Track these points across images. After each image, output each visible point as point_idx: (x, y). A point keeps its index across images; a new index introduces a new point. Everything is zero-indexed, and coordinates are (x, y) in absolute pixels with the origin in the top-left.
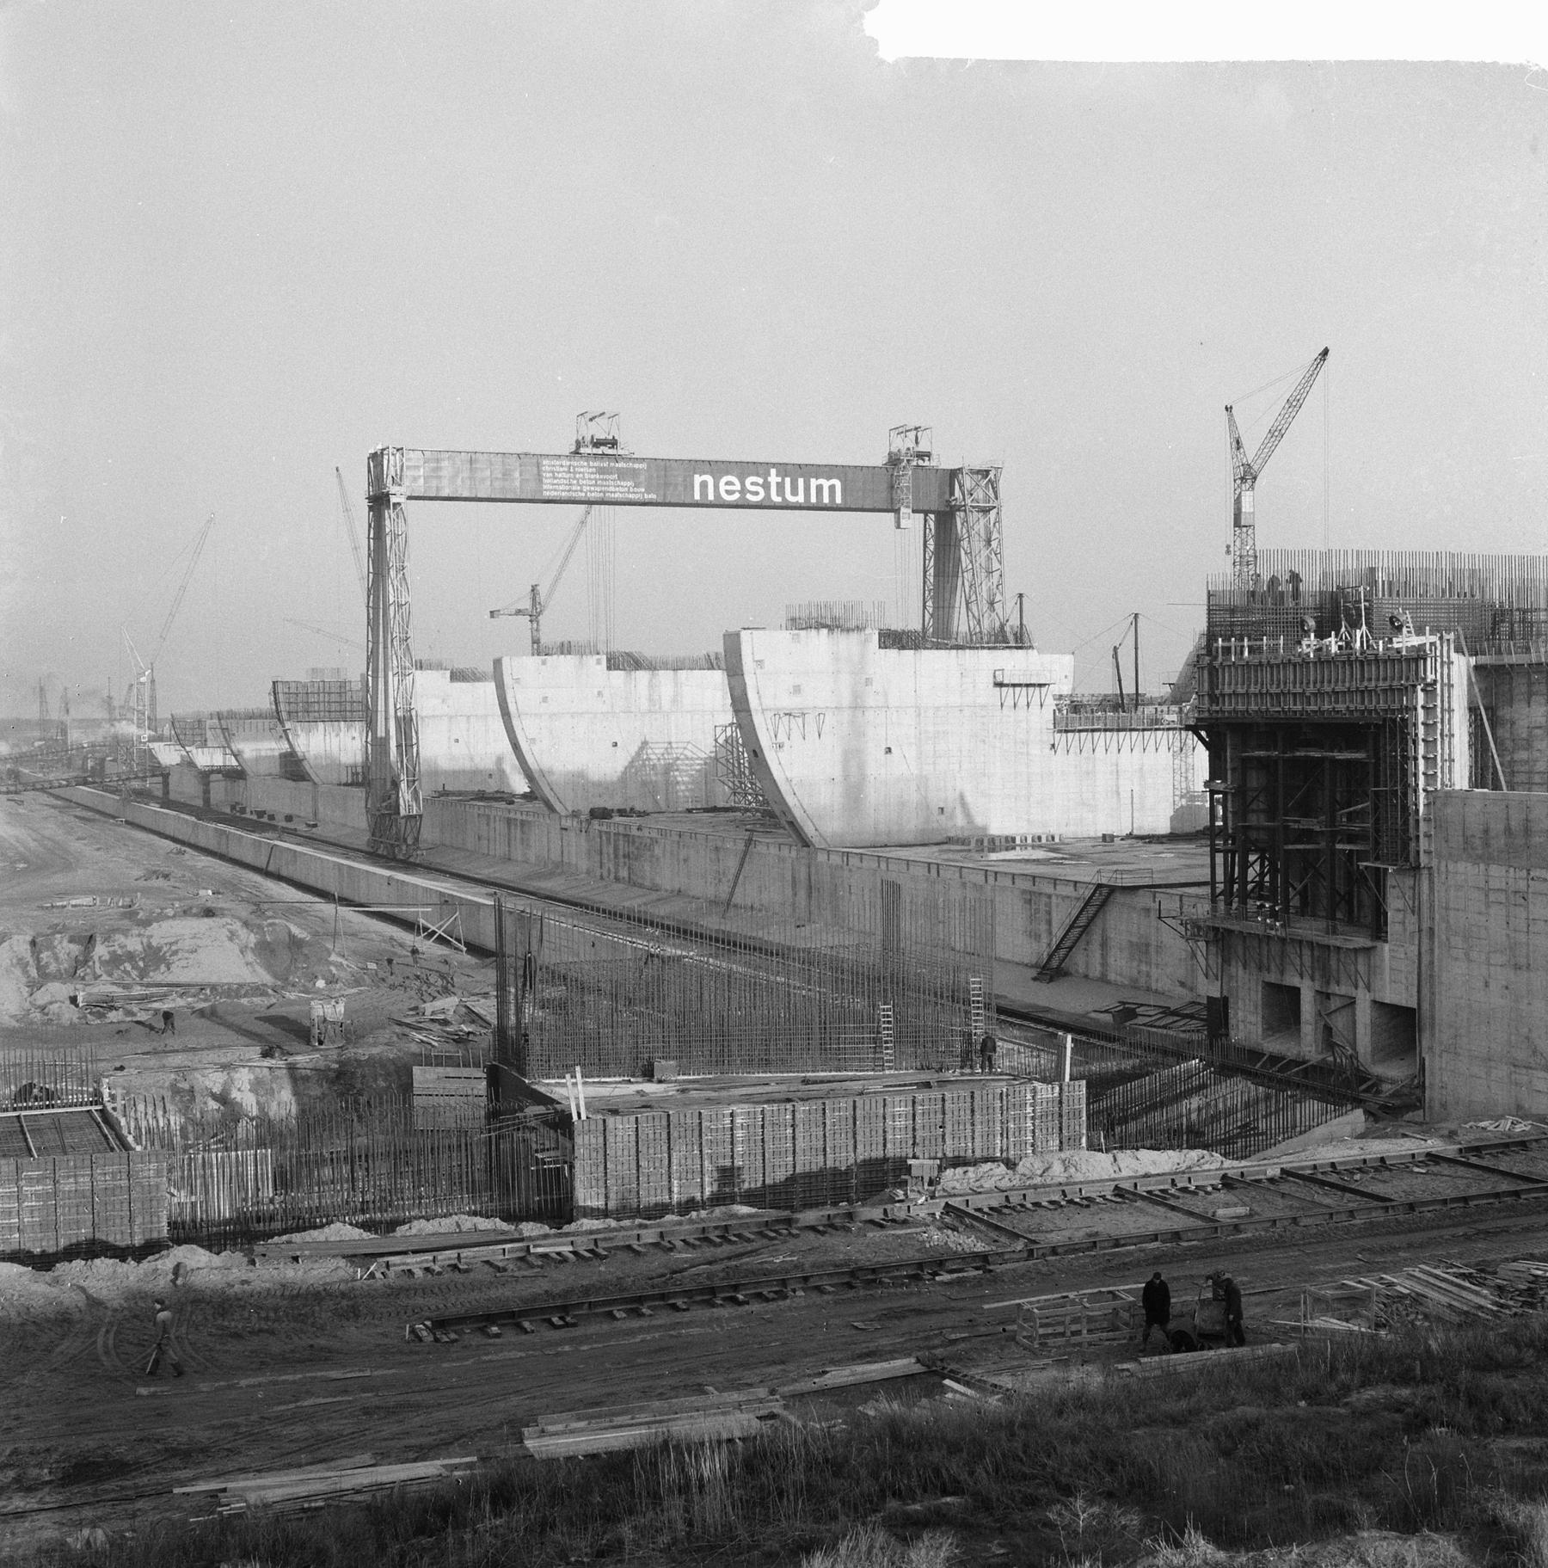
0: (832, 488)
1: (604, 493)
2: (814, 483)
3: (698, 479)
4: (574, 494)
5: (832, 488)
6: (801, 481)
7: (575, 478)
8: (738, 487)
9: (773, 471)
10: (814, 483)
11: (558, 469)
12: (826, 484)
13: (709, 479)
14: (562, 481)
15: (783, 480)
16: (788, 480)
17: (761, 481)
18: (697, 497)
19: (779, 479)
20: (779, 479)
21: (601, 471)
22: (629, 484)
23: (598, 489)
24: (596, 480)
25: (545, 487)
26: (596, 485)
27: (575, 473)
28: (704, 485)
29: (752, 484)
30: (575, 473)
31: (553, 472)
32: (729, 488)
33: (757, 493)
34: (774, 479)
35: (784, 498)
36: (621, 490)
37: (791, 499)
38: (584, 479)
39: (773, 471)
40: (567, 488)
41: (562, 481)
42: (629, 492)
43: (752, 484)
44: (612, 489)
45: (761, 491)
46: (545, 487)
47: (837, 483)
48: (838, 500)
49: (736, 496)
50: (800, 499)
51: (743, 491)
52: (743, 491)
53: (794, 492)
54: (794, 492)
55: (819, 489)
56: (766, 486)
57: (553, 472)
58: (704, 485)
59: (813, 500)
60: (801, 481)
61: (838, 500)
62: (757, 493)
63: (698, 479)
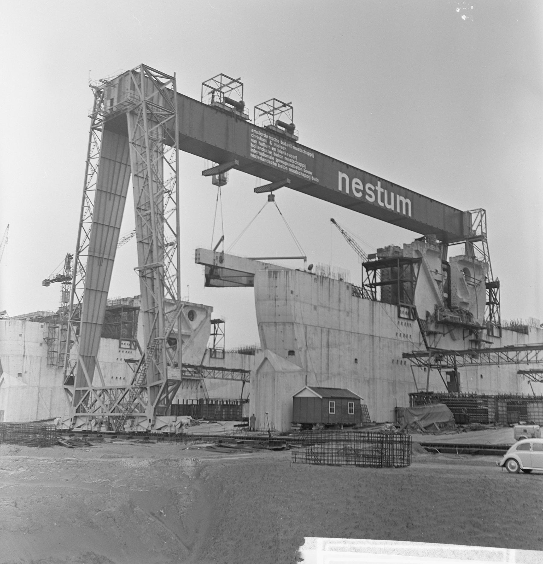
1: (288, 167)
3: (341, 175)
4: (270, 162)
7: (271, 150)
11: (260, 138)
13: (345, 175)
14: (263, 149)
22: (303, 165)
23: (285, 163)
24: (284, 156)
26: (284, 160)
28: (344, 179)
31: (258, 140)
38: (276, 152)
42: (303, 172)
44: (293, 166)
57: (258, 140)
58: (344, 179)
63: (341, 175)
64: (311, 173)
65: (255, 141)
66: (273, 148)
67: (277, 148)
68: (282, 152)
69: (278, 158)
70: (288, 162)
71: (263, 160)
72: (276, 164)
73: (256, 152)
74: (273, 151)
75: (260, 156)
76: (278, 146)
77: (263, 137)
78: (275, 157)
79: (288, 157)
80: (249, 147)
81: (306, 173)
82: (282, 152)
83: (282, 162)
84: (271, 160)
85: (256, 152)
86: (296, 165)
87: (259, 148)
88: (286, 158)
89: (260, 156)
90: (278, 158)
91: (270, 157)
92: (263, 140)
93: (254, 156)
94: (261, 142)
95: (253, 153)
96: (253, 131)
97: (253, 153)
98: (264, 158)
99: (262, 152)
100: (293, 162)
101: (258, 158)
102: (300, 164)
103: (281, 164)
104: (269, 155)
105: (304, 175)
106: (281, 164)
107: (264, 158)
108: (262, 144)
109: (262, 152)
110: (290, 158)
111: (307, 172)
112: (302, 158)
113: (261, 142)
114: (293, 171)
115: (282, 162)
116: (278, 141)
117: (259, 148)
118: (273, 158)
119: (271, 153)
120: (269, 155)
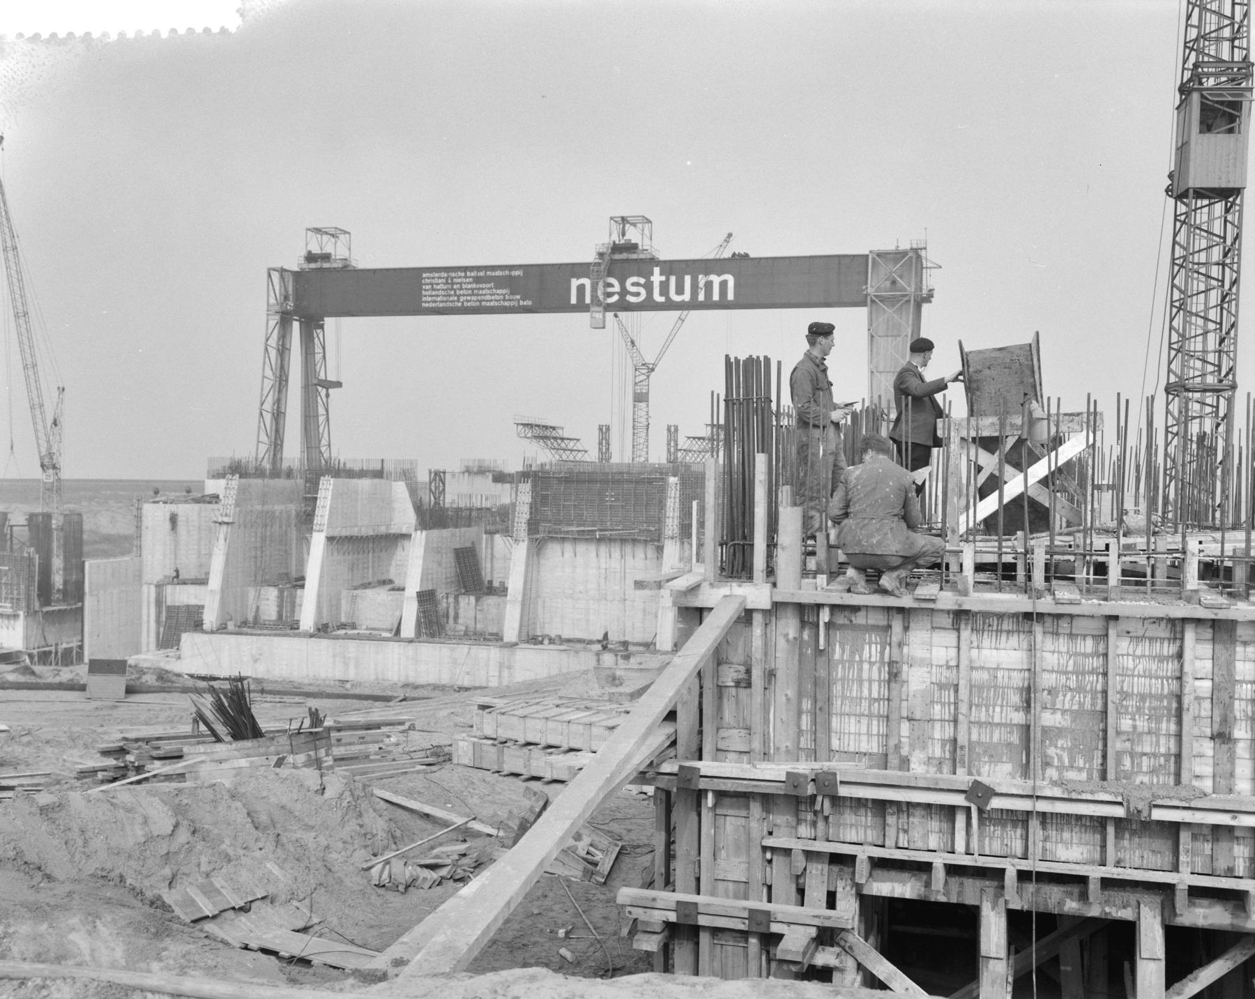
0: (724, 285)
2: (702, 280)
3: (575, 283)
5: (724, 285)
6: (688, 279)
7: (452, 289)
8: (617, 288)
9: (657, 270)
10: (702, 280)
11: (436, 281)
12: (716, 280)
14: (441, 293)
15: (668, 280)
16: (673, 279)
17: (642, 281)
18: (574, 300)
19: (663, 278)
20: (663, 278)
21: (477, 280)
22: (504, 291)
23: (474, 298)
24: (472, 290)
25: (424, 299)
26: (473, 295)
27: (453, 284)
28: (581, 289)
29: (634, 284)
30: (453, 284)
31: (432, 284)
32: (610, 290)
33: (638, 294)
34: (657, 278)
35: (668, 298)
36: (497, 297)
37: (677, 298)
38: (461, 289)
39: (657, 270)
40: (445, 299)
41: (441, 293)
42: (504, 300)
43: (634, 284)
44: (488, 297)
45: (643, 291)
46: (424, 299)
47: (730, 279)
48: (731, 296)
49: (615, 298)
50: (686, 297)
51: (624, 292)
52: (624, 292)
53: (680, 291)
54: (680, 291)
55: (709, 285)
56: (649, 287)
58: (581, 289)
59: (701, 297)
60: (688, 279)
61: (731, 296)
62: (638, 294)
63: (575, 283)
64: (518, 297)
65: (427, 287)
66: (455, 287)
67: (461, 284)
68: (469, 286)
69: (464, 295)
70: (478, 295)
71: (441, 305)
72: (460, 304)
73: (430, 299)
74: (455, 290)
75: (435, 302)
76: (459, 280)
77: (440, 278)
78: (459, 296)
79: (479, 289)
80: (421, 296)
81: (510, 300)
82: (469, 286)
83: (469, 298)
84: (453, 301)
85: (430, 299)
86: (491, 295)
87: (434, 293)
88: (475, 291)
89: (435, 302)
90: (464, 295)
91: (451, 299)
92: (440, 281)
93: (427, 305)
94: (437, 284)
95: (425, 302)
96: (424, 275)
97: (425, 302)
98: (442, 302)
99: (437, 296)
100: (488, 292)
101: (434, 305)
102: (499, 291)
103: (468, 301)
104: (450, 296)
105: (506, 304)
106: (468, 301)
107: (442, 302)
108: (439, 287)
109: (437, 296)
110: (482, 289)
111: (511, 297)
112: (499, 283)
113: (437, 284)
114: (488, 304)
115: (469, 298)
116: (463, 274)
117: (434, 293)
118: (456, 298)
119: (452, 292)
120: (450, 296)
